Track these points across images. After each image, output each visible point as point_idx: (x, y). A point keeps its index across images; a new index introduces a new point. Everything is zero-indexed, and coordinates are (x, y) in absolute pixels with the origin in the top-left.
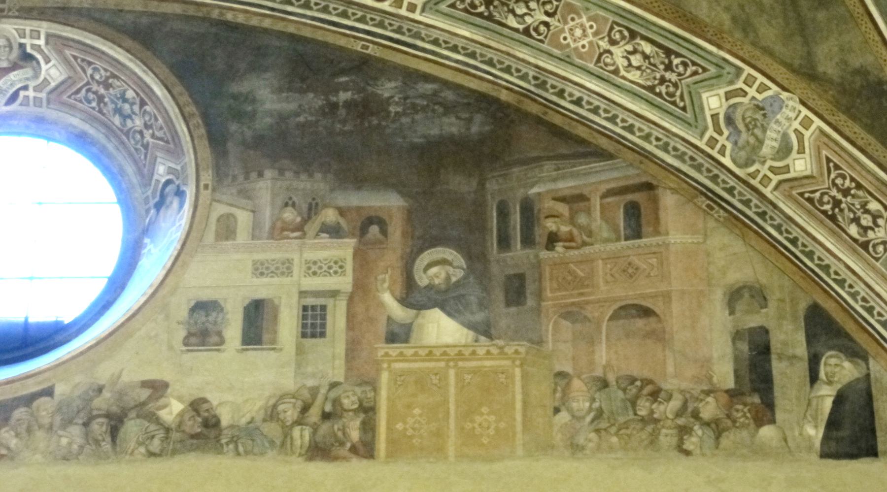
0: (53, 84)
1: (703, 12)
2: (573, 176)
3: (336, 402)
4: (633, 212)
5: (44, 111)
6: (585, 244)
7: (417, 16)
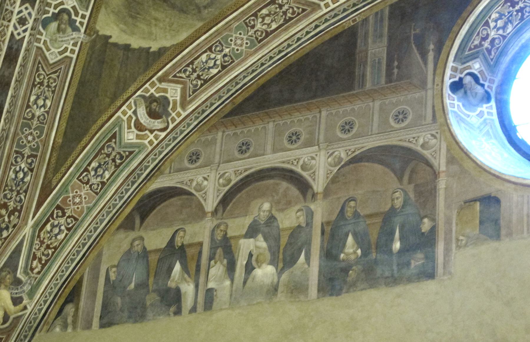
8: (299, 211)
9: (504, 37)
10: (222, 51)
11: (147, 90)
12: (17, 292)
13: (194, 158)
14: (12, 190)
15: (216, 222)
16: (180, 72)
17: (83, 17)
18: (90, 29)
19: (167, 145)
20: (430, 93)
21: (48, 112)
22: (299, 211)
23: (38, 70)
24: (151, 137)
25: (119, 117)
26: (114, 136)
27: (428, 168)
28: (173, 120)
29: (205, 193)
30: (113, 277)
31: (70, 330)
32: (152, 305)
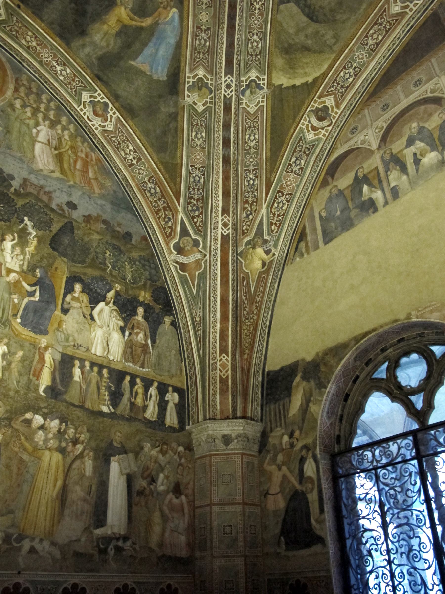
8: (439, 114)
10: (352, 66)
11: (313, 106)
12: (266, 247)
13: (354, 131)
14: (248, 192)
15: (382, 152)
16: (330, 88)
17: (264, 80)
18: (270, 85)
19: (335, 132)
21: (258, 142)
22: (439, 114)
23: (246, 120)
24: (323, 132)
25: (301, 128)
26: (301, 139)
28: (334, 117)
29: (369, 142)
30: (324, 214)
31: (305, 256)
32: (355, 216)
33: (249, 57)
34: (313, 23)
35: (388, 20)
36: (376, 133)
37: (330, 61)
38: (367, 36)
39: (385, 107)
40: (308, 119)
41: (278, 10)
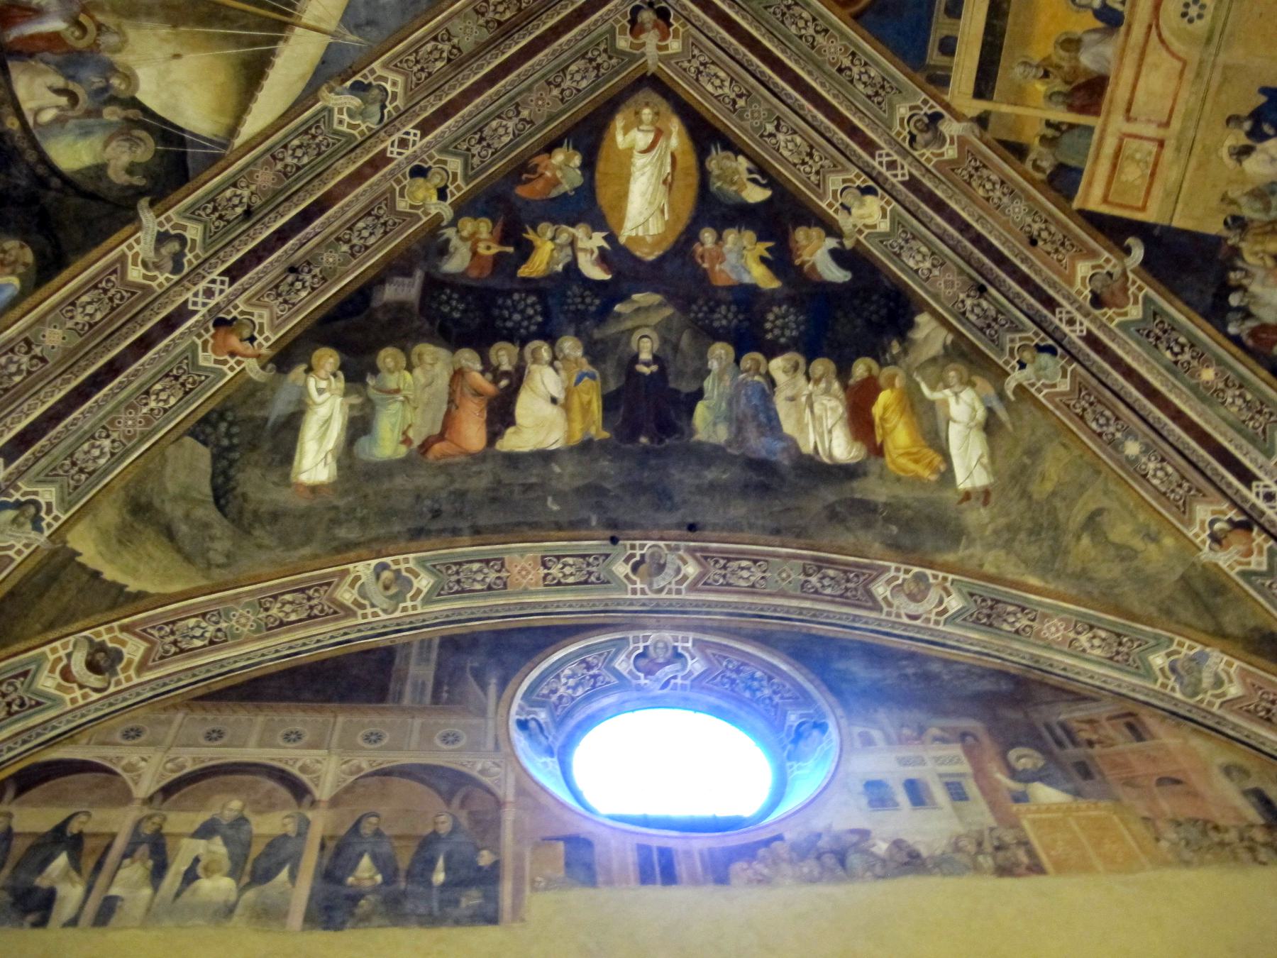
0: (696, 674)
1: (1137, 607)
2: (1081, 710)
3: (999, 838)
4: (1131, 727)
5: (688, 693)
6: (1112, 745)
7: (941, 627)
8: (287, 817)
9: (573, 699)
10: (217, 623)
11: (99, 634)
13: (133, 734)
15: (147, 811)
17: (56, 518)
18: (58, 535)
19: (96, 710)
20: (491, 723)
22: (287, 817)
24: (78, 693)
25: (44, 654)
26: (25, 674)
27: (488, 796)
28: (118, 683)
29: (140, 776)
33: (68, 462)
34: (212, 507)
35: (324, 601)
36: (164, 768)
37: (193, 585)
38: (275, 597)
39: (214, 736)
40: (70, 649)
41: (177, 439)
